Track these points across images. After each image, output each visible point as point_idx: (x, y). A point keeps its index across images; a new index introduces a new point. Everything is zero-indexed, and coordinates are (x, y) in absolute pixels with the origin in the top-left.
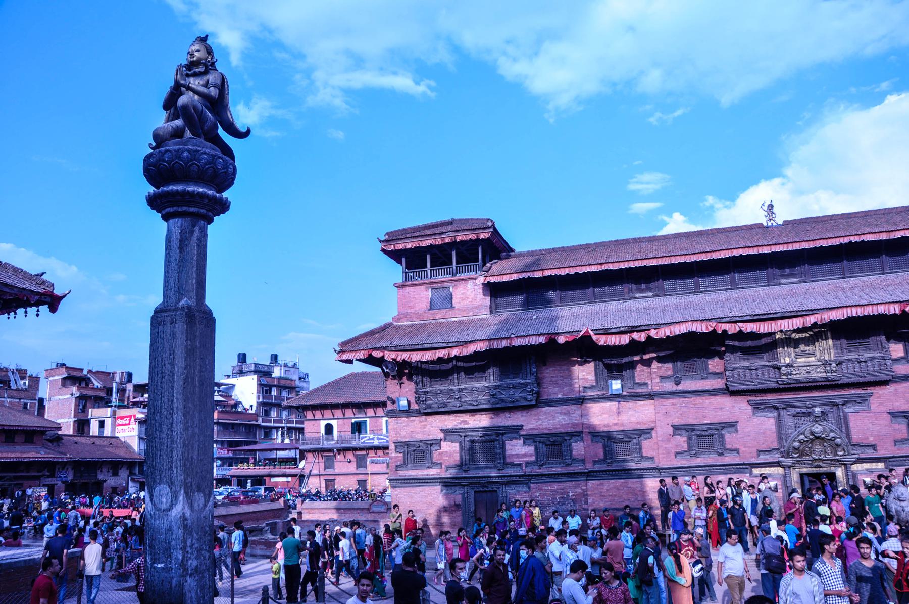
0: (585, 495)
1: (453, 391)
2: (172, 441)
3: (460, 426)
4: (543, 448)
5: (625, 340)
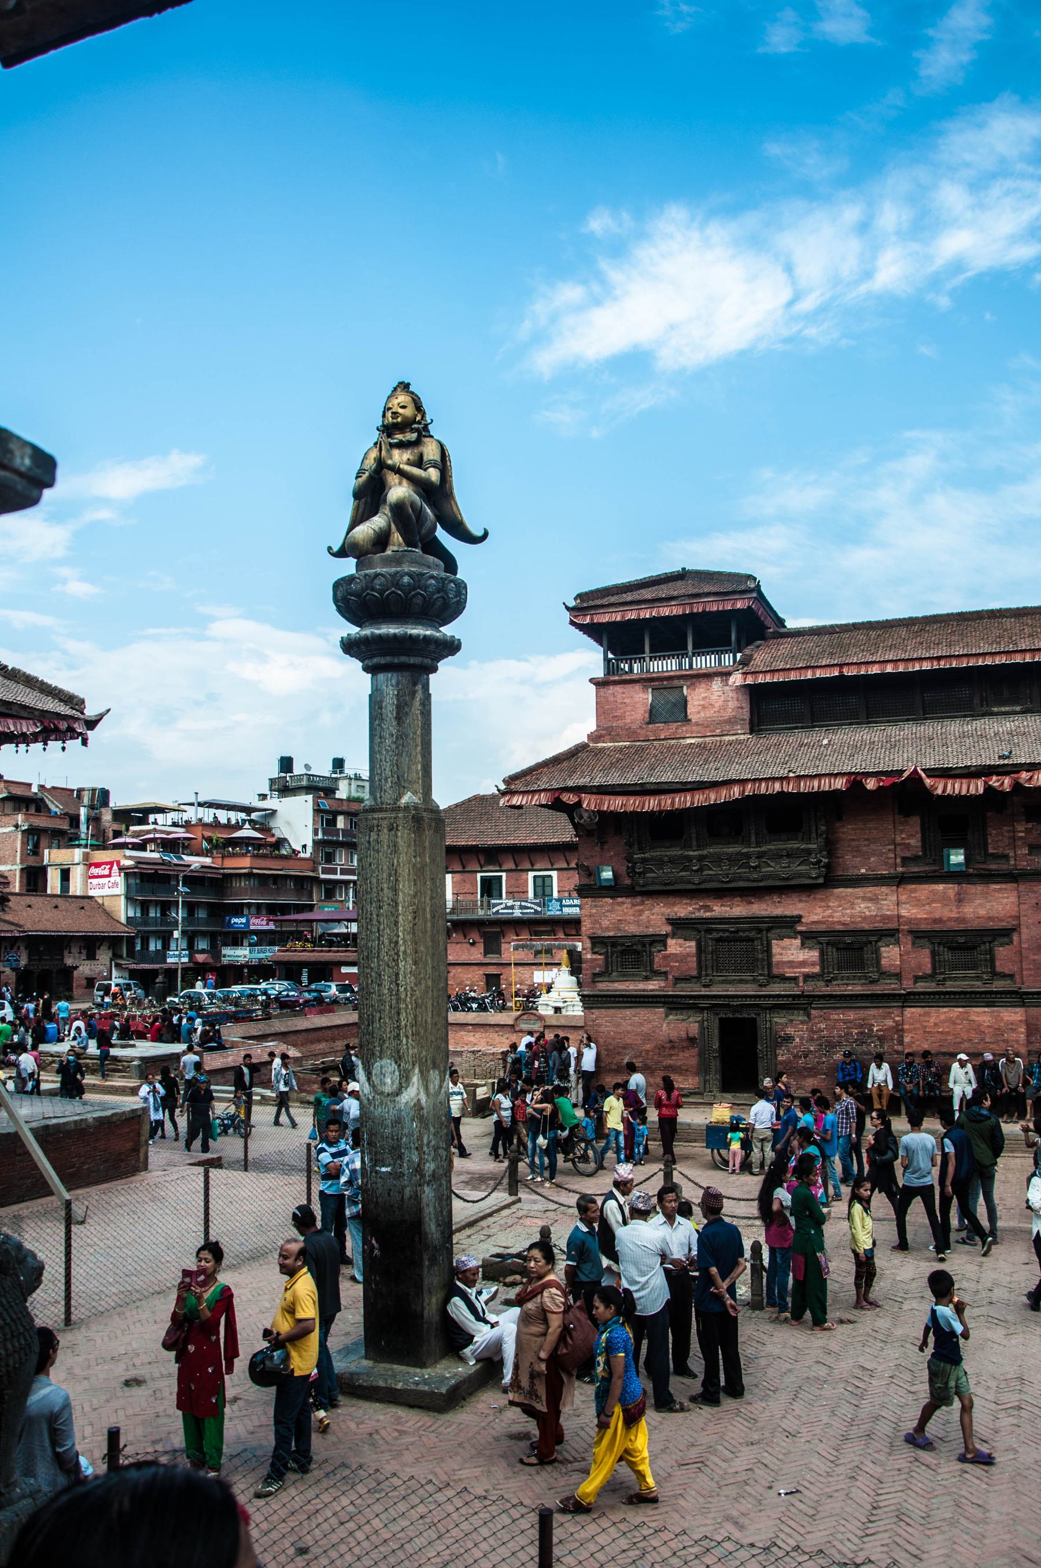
0: (899, 1029)
1: (689, 859)
2: (398, 1000)
4: (833, 953)
5: (977, 787)
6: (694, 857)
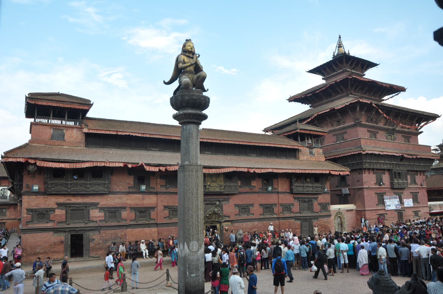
0: (125, 235)
1: (67, 184)
2: (198, 223)
3: (66, 202)
5: (157, 169)
6: (69, 184)
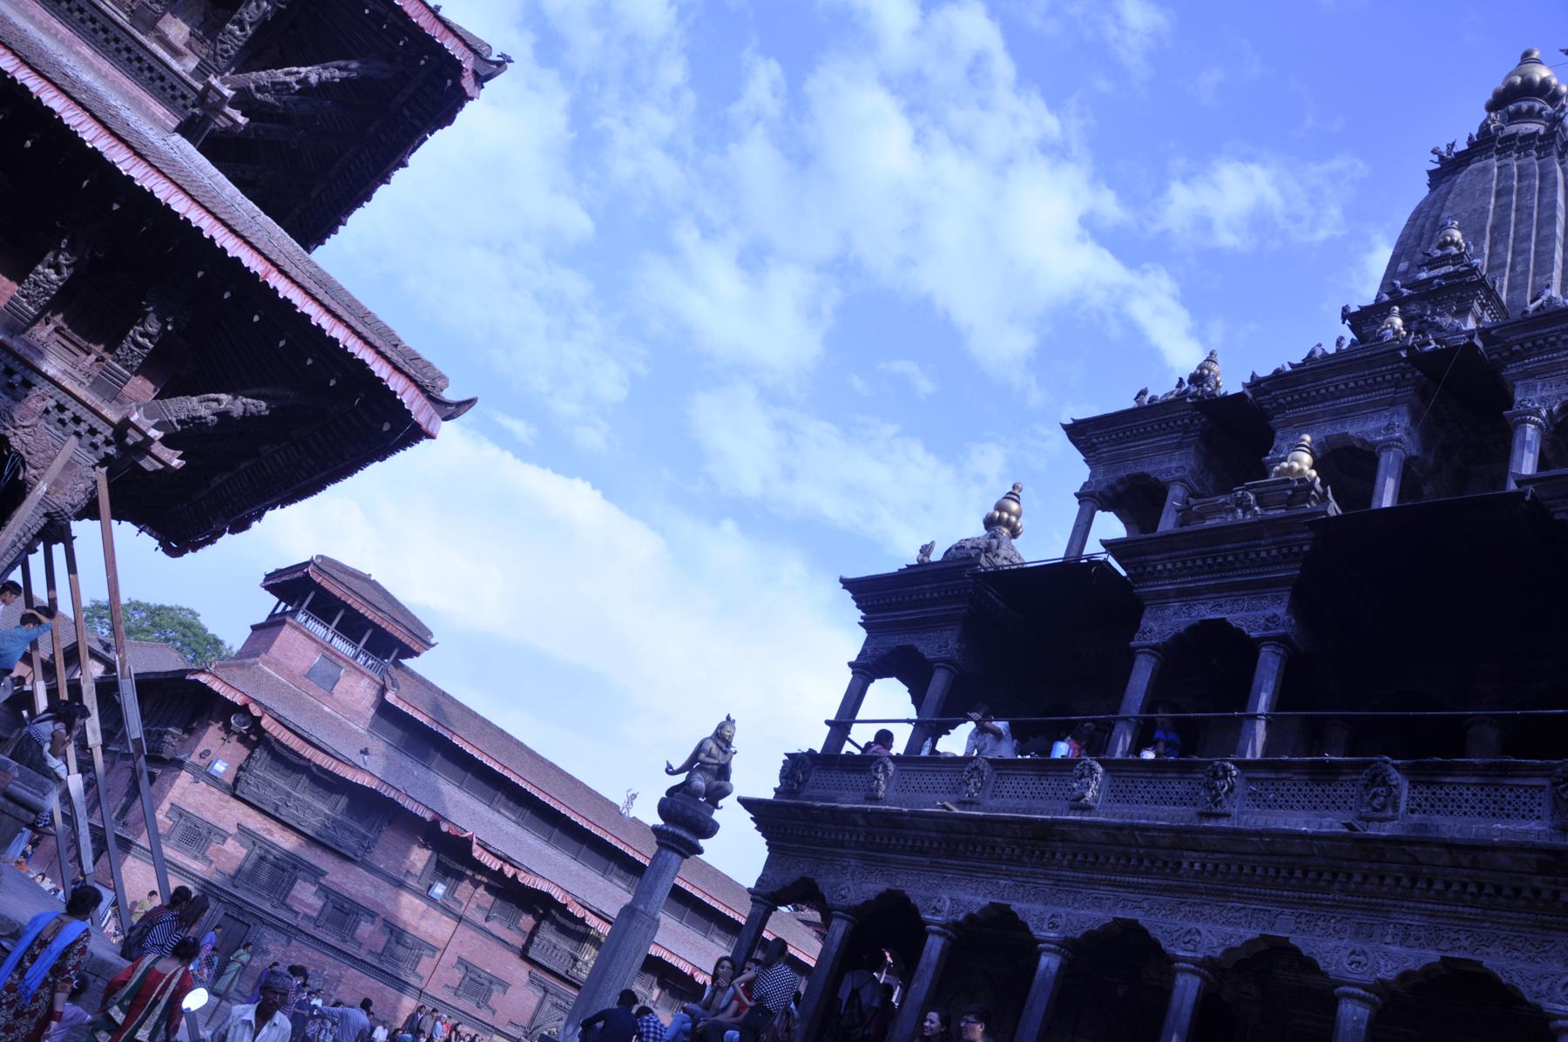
5: (495, 865)
